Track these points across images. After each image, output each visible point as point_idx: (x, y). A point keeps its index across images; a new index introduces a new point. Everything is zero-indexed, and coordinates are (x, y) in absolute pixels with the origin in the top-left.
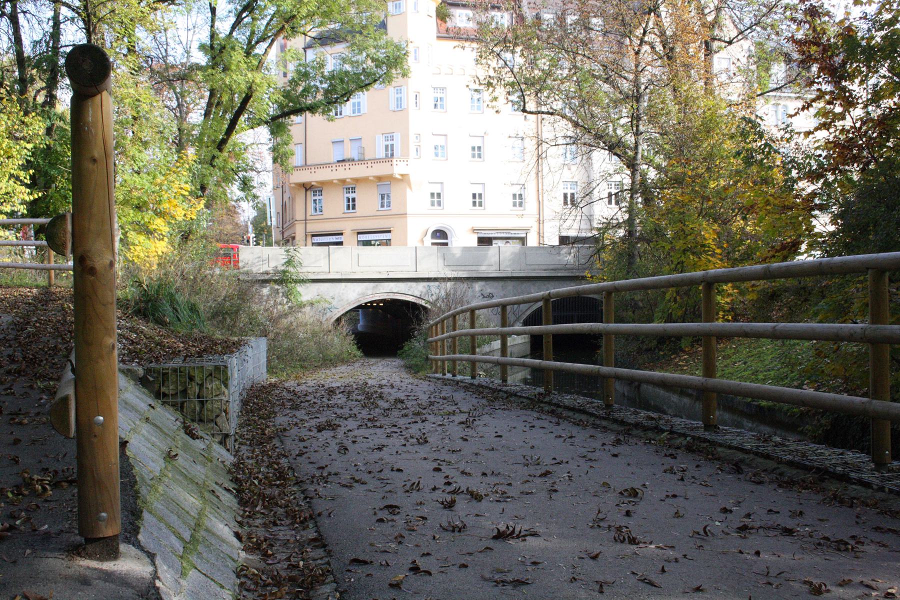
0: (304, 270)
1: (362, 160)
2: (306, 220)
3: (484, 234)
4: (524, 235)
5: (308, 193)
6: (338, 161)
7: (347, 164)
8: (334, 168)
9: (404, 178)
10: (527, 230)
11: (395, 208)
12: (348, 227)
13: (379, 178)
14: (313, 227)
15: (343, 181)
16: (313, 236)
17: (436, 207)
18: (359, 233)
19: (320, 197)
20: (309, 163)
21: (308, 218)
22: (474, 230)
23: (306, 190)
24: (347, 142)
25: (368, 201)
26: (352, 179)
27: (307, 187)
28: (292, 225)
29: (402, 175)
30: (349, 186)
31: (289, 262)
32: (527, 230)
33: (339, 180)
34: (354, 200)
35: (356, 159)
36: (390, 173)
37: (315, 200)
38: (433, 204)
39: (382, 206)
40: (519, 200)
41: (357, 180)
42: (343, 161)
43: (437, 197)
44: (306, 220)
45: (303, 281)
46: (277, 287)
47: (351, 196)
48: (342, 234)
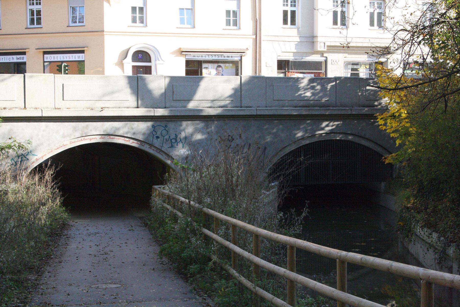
3: (191, 57)
4: (237, 59)
10: (242, 53)
11: (88, 24)
12: (32, 43)
17: (138, 24)
18: (45, 53)
22: (182, 52)
32: (242, 53)
34: (39, 12)
38: (134, 21)
40: (233, 18)
43: (139, 14)
48: (24, 53)
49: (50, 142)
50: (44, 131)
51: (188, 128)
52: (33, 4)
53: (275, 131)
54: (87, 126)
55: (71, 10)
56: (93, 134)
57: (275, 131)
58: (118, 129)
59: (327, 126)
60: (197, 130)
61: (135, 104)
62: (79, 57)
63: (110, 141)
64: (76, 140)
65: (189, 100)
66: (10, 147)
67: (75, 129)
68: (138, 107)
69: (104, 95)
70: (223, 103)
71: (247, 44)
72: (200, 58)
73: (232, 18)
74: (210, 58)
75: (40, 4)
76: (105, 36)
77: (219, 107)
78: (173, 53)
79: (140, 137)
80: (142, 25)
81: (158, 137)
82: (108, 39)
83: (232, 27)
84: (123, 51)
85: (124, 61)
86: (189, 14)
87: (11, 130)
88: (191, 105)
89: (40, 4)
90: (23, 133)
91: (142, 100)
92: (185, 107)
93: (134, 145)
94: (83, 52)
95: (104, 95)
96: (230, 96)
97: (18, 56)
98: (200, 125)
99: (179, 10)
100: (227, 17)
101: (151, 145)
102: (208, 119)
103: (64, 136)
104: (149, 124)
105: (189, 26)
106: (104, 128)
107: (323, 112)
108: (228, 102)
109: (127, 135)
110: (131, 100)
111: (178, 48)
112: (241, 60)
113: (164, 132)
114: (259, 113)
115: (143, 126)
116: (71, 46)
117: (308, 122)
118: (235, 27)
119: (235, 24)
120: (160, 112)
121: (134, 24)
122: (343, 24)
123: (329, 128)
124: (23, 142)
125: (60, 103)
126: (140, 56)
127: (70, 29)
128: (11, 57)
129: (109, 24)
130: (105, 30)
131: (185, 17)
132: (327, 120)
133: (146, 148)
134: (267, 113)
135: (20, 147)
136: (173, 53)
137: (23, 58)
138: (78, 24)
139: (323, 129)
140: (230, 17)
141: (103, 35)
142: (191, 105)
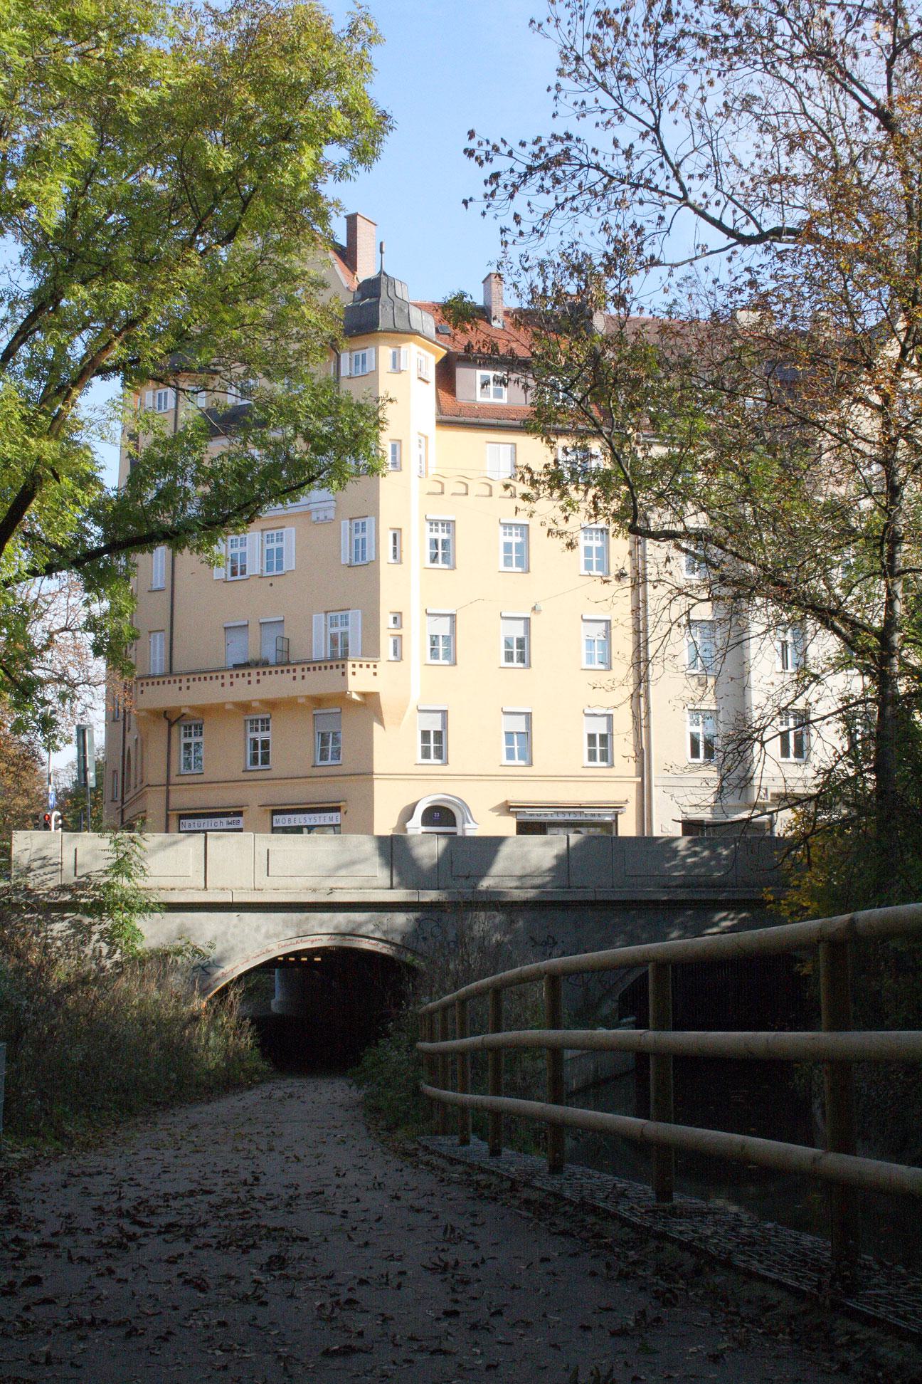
0: (150, 883)
1: (285, 662)
2: (168, 784)
5: (175, 729)
6: (236, 666)
7: (254, 672)
8: (227, 680)
9: (370, 702)
10: (617, 809)
11: (348, 761)
12: (254, 796)
13: (318, 701)
14: (184, 798)
15: (245, 707)
16: (182, 817)
17: (433, 760)
18: (275, 812)
19: (199, 739)
20: (176, 669)
21: (174, 780)
22: (507, 808)
23: (171, 725)
24: (254, 628)
25: (292, 746)
26: (262, 702)
27: (171, 718)
28: (140, 796)
29: (364, 695)
30: (257, 716)
31: (120, 867)
32: (617, 809)
33: (236, 704)
34: (266, 744)
35: (272, 660)
36: (340, 690)
37: (187, 746)
38: (426, 754)
39: (324, 758)
40: (601, 746)
41: (272, 705)
42: (246, 665)
43: (436, 744)
44: (168, 784)
45: (148, 908)
46: (87, 920)
47: (260, 736)
48: (240, 814)
49: (248, 945)
50: (235, 926)
51: (482, 923)
52: (257, 730)
53: (629, 928)
54: (307, 919)
55: (318, 740)
56: (319, 933)
57: (629, 928)
58: (360, 925)
59: (724, 919)
60: (496, 928)
61: (387, 883)
62: (331, 819)
63: (346, 944)
64: (289, 942)
65: (483, 875)
66: (179, 952)
67: (286, 924)
68: (391, 888)
69: (339, 867)
70: (538, 881)
71: (626, 792)
72: (542, 819)
73: (598, 748)
74: (561, 818)
75: (268, 729)
76: (376, 783)
77: (532, 888)
78: (494, 810)
79: (398, 940)
80: (439, 761)
81: (425, 939)
82: (379, 787)
83: (599, 763)
84: (407, 807)
85: (409, 825)
86: (521, 744)
87: (182, 924)
88: (485, 883)
89: (268, 729)
91: (400, 874)
92: (474, 887)
93: (385, 951)
94: (337, 809)
95: (339, 867)
96: (550, 870)
97: (230, 819)
98: (499, 918)
99: (504, 736)
100: (590, 745)
101: (414, 952)
102: (512, 908)
103: (268, 936)
104: (412, 916)
105: (523, 763)
106: (335, 922)
107: (713, 897)
108: (548, 879)
110: (381, 875)
111: (503, 800)
112: (616, 821)
113: (437, 931)
114: (599, 898)
115: (401, 919)
116: (317, 799)
117: (690, 912)
118: (604, 764)
119: (604, 757)
120: (430, 896)
121: (426, 761)
122: (799, 753)
123: (728, 923)
124: (201, 944)
125: (262, 881)
126: (437, 815)
127: (316, 771)
128: (218, 820)
129: (382, 760)
130: (376, 771)
131: (516, 747)
132: (727, 909)
133: (409, 958)
134: (613, 898)
135: (196, 951)
136: (494, 810)
137: (238, 822)
138: (330, 762)
139: (716, 924)
140: (594, 745)
141: (372, 780)
142: (485, 883)
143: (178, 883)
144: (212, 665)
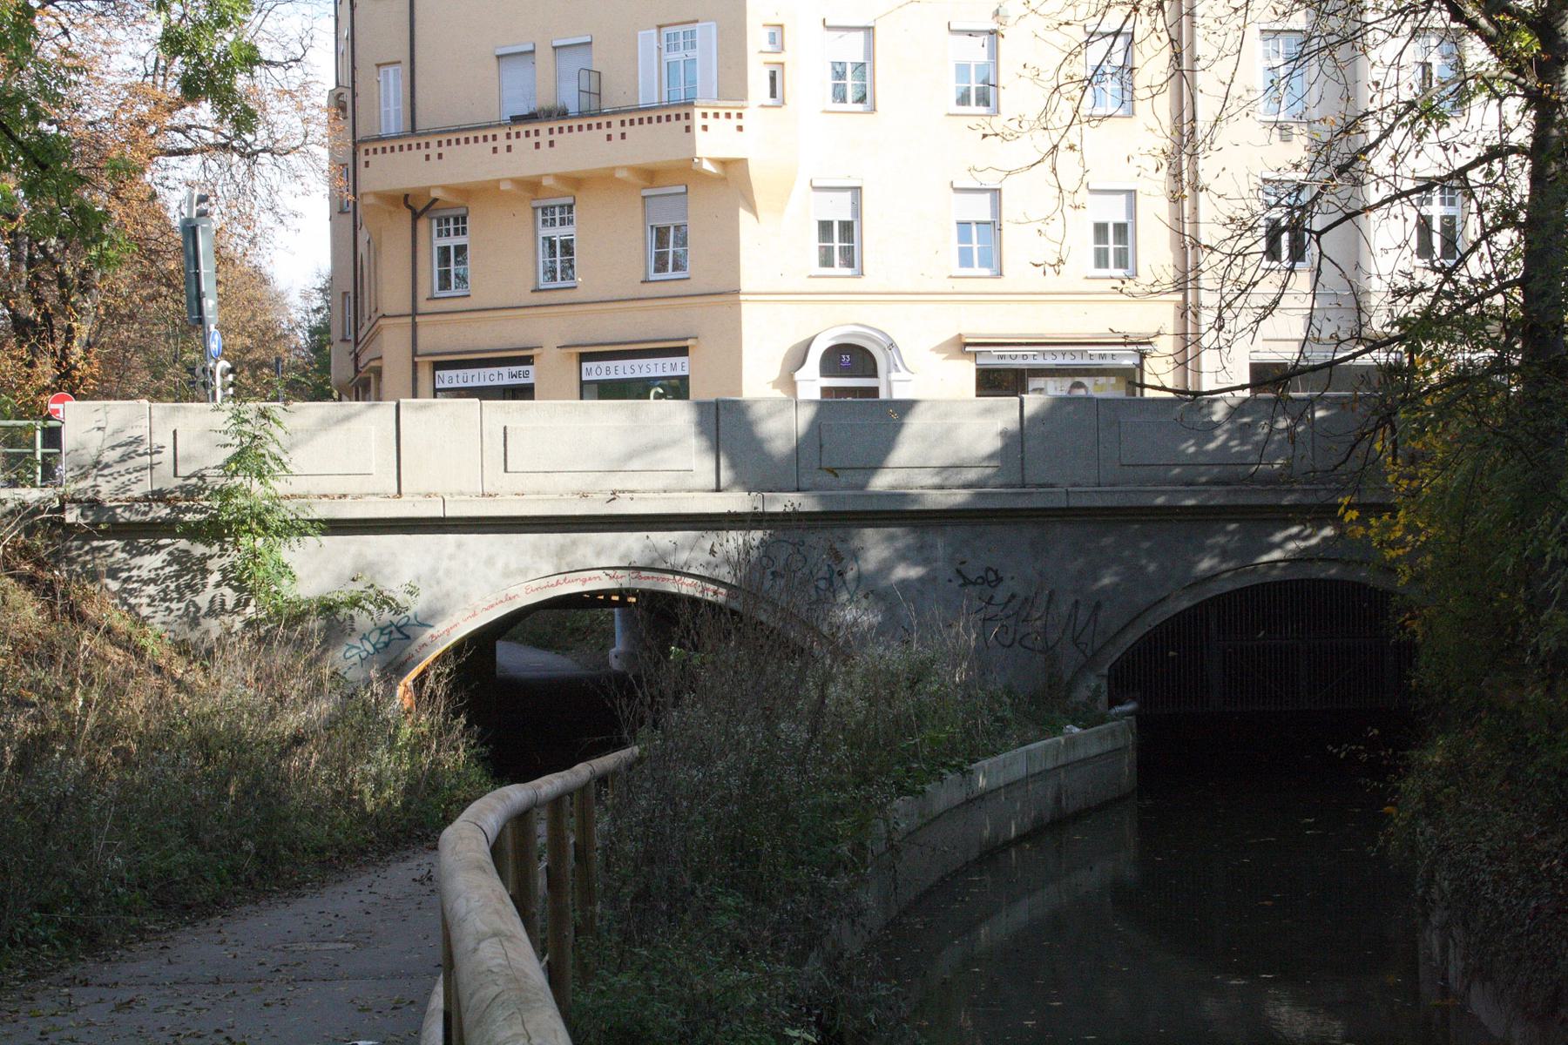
0: (298, 486)
1: (593, 111)
2: (415, 313)
3: (992, 359)
4: (1128, 362)
5: (423, 224)
6: (516, 120)
7: (544, 128)
8: (502, 143)
9: (733, 172)
10: (1141, 346)
11: (699, 270)
12: (549, 332)
13: (650, 175)
14: (439, 336)
15: (532, 186)
16: (438, 366)
18: (584, 357)
19: (460, 240)
20: (422, 124)
21: (423, 306)
22: (963, 347)
23: (416, 216)
24: (544, 57)
25: (611, 248)
26: (559, 178)
27: (417, 207)
28: (375, 333)
29: (723, 163)
30: (552, 201)
31: (247, 458)
33: (517, 182)
34: (567, 248)
35: (573, 109)
36: (686, 156)
37: (445, 251)
38: (826, 261)
39: (661, 266)
40: (1115, 241)
41: (576, 182)
42: (532, 117)
43: (841, 241)
44: (415, 313)
45: (295, 528)
46: (199, 549)
47: (559, 233)
48: (528, 360)
49: (474, 588)
50: (452, 557)
51: (872, 547)
52: (553, 224)
54: (574, 543)
55: (652, 237)
56: (597, 564)
60: (903, 557)
62: (674, 367)
64: (543, 582)
65: (875, 467)
66: (355, 603)
68: (718, 490)
69: (630, 456)
70: (971, 475)
71: (1155, 317)
72: (1019, 363)
74: (1050, 362)
75: (571, 222)
76: (745, 307)
77: (964, 487)
78: (939, 349)
80: (848, 271)
82: (751, 315)
84: (795, 347)
85: (798, 375)
86: (983, 240)
88: (882, 482)
89: (571, 222)
90: (405, 565)
91: (733, 465)
92: (863, 487)
94: (683, 351)
95: (630, 456)
96: (991, 457)
97: (515, 369)
98: (903, 537)
99: (954, 228)
103: (507, 574)
105: (986, 272)
106: (622, 548)
107: (1270, 499)
109: (697, 567)
114: (1074, 503)
117: (1232, 527)
119: (1122, 261)
120: (781, 503)
125: (496, 480)
126: (846, 358)
127: (649, 290)
128: (494, 370)
130: (744, 288)
131: (975, 246)
134: (1099, 503)
135: (384, 601)
136: (939, 349)
137: (526, 374)
139: (1280, 545)
141: (738, 303)
142: (882, 482)
143: (351, 485)
144: (481, 119)
